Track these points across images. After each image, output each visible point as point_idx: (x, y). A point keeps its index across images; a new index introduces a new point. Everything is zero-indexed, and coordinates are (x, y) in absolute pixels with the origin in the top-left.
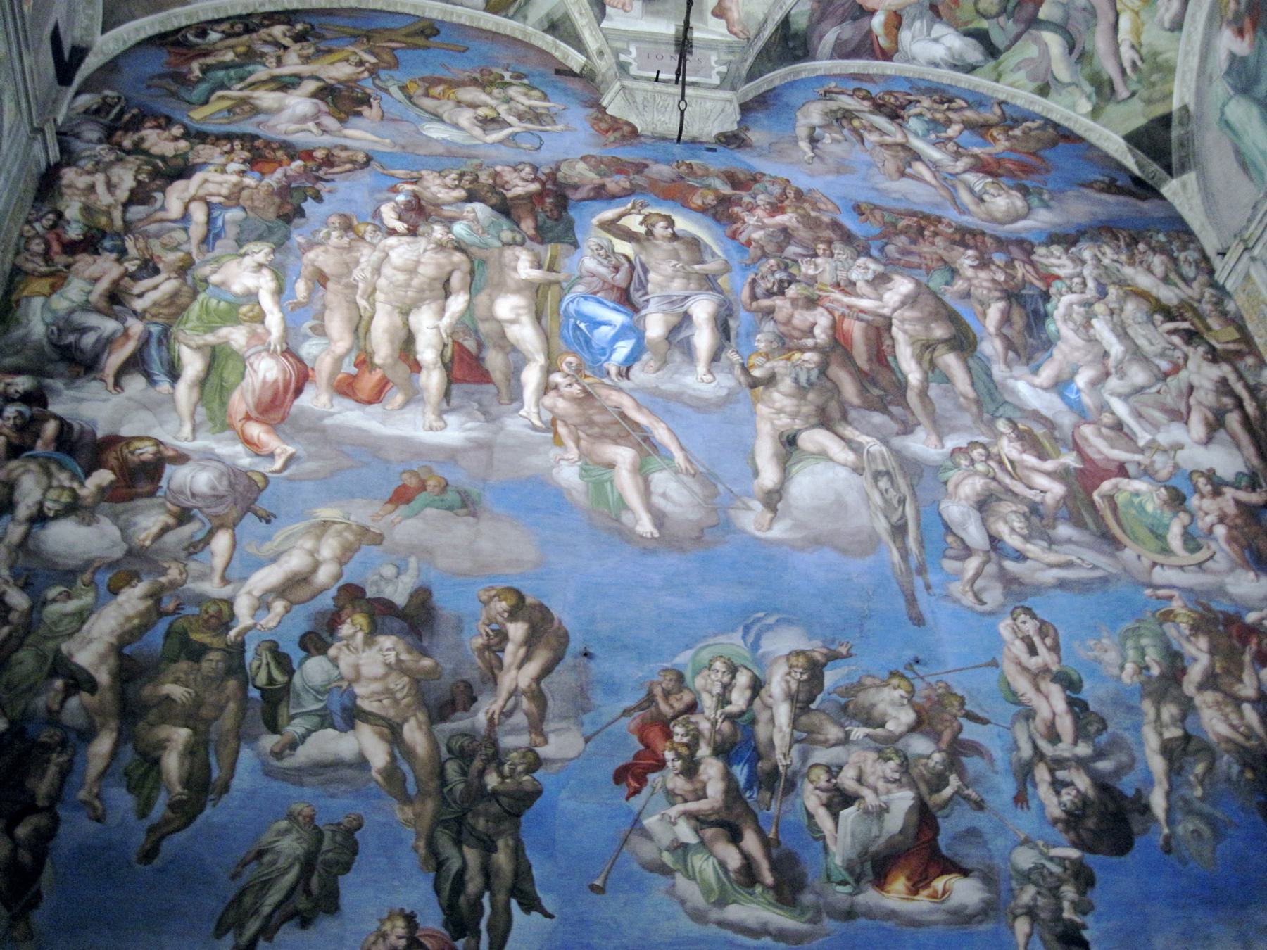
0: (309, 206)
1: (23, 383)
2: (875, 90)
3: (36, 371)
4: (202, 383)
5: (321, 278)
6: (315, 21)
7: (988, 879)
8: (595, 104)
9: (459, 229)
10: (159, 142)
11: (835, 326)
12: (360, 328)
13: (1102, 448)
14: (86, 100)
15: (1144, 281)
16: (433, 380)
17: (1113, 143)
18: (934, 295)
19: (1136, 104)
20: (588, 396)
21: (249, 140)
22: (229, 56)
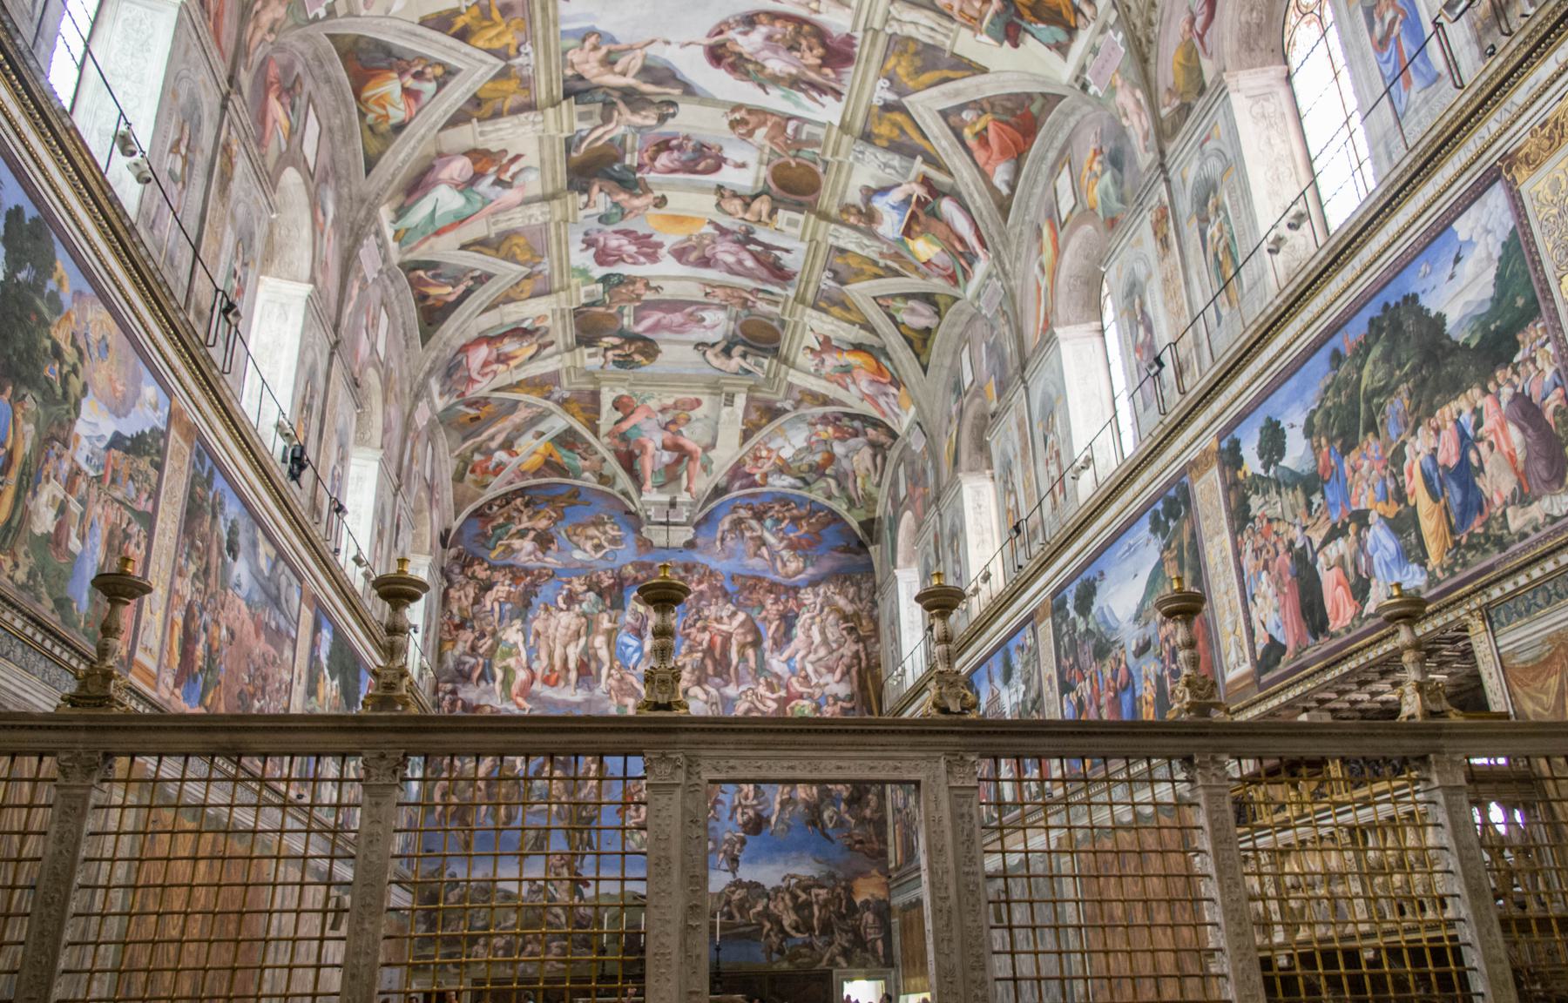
0: (533, 600)
1: (449, 686)
2: (756, 503)
3: (452, 681)
4: (503, 682)
5: (538, 634)
6: (532, 493)
7: (715, 842)
8: (637, 531)
9: (584, 605)
10: (481, 572)
11: (711, 641)
12: (551, 656)
13: (796, 686)
14: (453, 552)
15: (841, 602)
16: (573, 675)
17: (855, 525)
18: (752, 620)
19: (863, 512)
20: (622, 678)
21: (511, 566)
22: (501, 520)
